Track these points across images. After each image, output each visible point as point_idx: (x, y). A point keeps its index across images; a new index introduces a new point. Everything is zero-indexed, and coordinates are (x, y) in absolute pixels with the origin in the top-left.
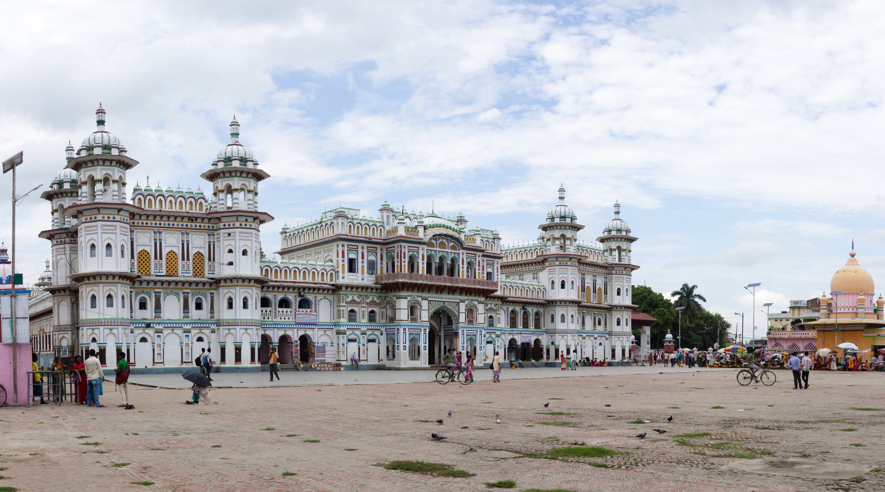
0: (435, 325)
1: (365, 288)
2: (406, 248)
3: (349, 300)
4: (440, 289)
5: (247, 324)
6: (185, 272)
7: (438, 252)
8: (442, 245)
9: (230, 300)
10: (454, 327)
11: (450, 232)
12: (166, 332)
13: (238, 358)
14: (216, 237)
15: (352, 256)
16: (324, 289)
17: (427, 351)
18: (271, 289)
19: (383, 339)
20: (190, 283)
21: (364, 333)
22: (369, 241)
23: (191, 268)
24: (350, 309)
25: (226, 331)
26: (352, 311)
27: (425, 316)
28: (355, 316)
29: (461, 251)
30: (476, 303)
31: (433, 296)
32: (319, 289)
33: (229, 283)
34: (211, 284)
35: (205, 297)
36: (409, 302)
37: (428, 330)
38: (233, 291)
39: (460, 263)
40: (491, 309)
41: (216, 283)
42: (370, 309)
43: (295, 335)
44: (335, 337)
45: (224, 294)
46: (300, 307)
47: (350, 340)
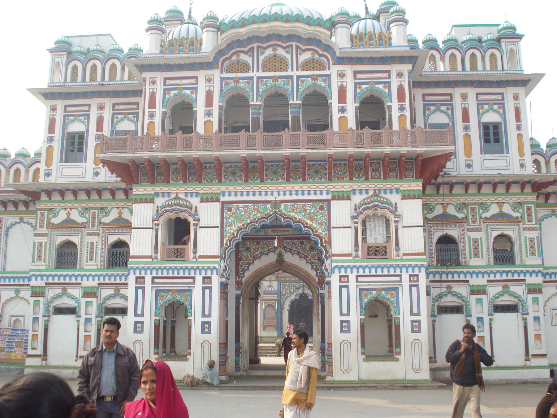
0: (308, 268)
2: (156, 84)
3: (62, 216)
7: (256, 81)
8: (276, 63)
15: (76, 127)
16: (15, 204)
17: (214, 337)
21: (89, 293)
24: (60, 239)
26: (70, 244)
28: (76, 254)
29: (334, 70)
30: (395, 198)
31: (234, 191)
40: (501, 217)
42: (112, 239)
47: (60, 311)
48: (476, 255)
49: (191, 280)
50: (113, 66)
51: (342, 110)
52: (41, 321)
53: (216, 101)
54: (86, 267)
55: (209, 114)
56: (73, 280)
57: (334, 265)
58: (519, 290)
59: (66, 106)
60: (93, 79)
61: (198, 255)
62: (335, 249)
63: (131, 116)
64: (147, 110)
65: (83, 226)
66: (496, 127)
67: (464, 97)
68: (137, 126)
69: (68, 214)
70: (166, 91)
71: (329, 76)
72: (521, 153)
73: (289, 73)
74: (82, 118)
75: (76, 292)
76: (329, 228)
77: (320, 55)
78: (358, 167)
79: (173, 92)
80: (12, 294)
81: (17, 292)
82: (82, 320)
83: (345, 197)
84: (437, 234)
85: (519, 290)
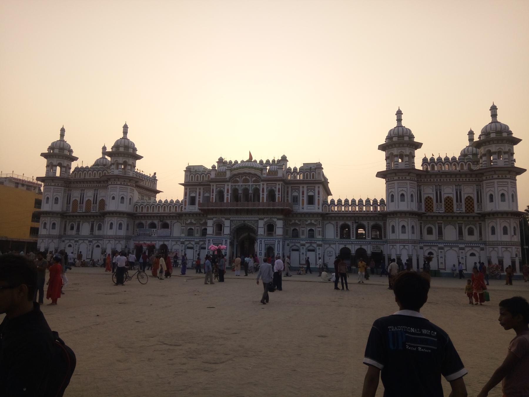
3: (189, 221)
4: (238, 212)
5: (110, 238)
6: (95, 210)
7: (240, 186)
9: (112, 224)
11: (253, 171)
12: (80, 242)
15: (193, 195)
16: (176, 217)
21: (197, 243)
22: (200, 184)
24: (189, 228)
26: (191, 229)
29: (261, 183)
30: (275, 220)
37: (228, 241)
42: (203, 228)
48: (303, 235)
50: (203, 176)
51: (263, 195)
52: (184, 251)
53: (230, 192)
55: (228, 195)
58: (315, 245)
60: (197, 180)
62: (259, 233)
65: (195, 224)
66: (313, 196)
67: (303, 187)
70: (216, 188)
72: (319, 205)
75: (193, 243)
76: (258, 228)
78: (265, 212)
81: (177, 242)
83: (262, 219)
84: (292, 228)
85: (315, 245)
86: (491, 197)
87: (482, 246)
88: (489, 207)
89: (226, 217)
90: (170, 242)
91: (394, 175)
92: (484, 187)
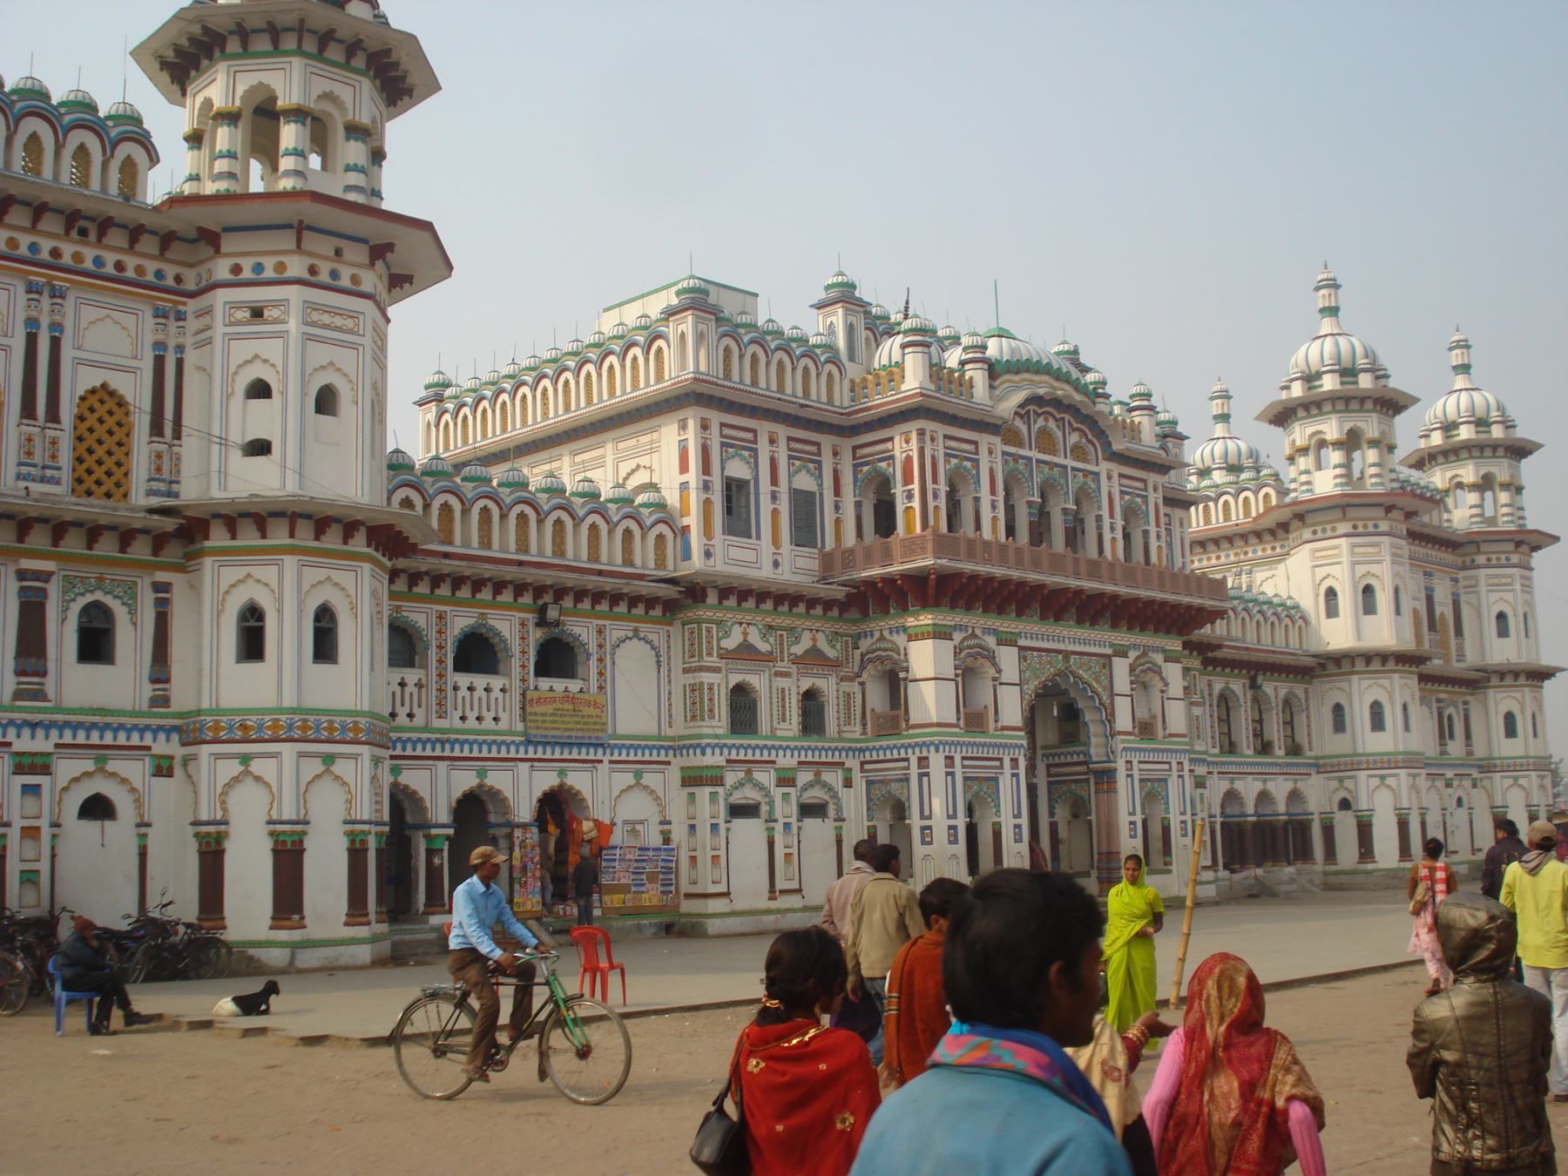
1: (786, 599)
8: (1045, 442)
10: (1096, 751)
13: (288, 898)
14: (192, 324)
16: (634, 601)
18: (423, 588)
19: (854, 802)
20: (59, 530)
23: (65, 457)
24: (735, 679)
25: (235, 768)
27: (1012, 710)
29: (1104, 467)
30: (1158, 658)
31: (1036, 632)
32: (615, 599)
33: (249, 537)
34: (159, 541)
35: (130, 597)
36: (957, 651)
38: (269, 573)
39: (1105, 513)
41: (187, 533)
42: (806, 684)
43: (521, 790)
44: (677, 798)
45: (223, 584)
46: (543, 670)
47: (740, 811)
49: (997, 763)
51: (1112, 529)
54: (779, 733)
56: (766, 757)
57: (1121, 746)
59: (723, 425)
61: (1000, 724)
63: (811, 466)
64: (930, 485)
65: (768, 658)
68: (820, 485)
69: (745, 634)
71: (1097, 474)
73: (1060, 460)
74: (746, 453)
75: (766, 777)
76: (1112, 695)
77: (1090, 441)
79: (954, 461)
80: (629, 779)
81: (638, 775)
82: (779, 827)
83: (1122, 653)
86: (1501, 617)
87: (1475, 774)
88: (1502, 652)
89: (1008, 625)
90: (604, 767)
91: (1380, 512)
92: (1483, 588)
